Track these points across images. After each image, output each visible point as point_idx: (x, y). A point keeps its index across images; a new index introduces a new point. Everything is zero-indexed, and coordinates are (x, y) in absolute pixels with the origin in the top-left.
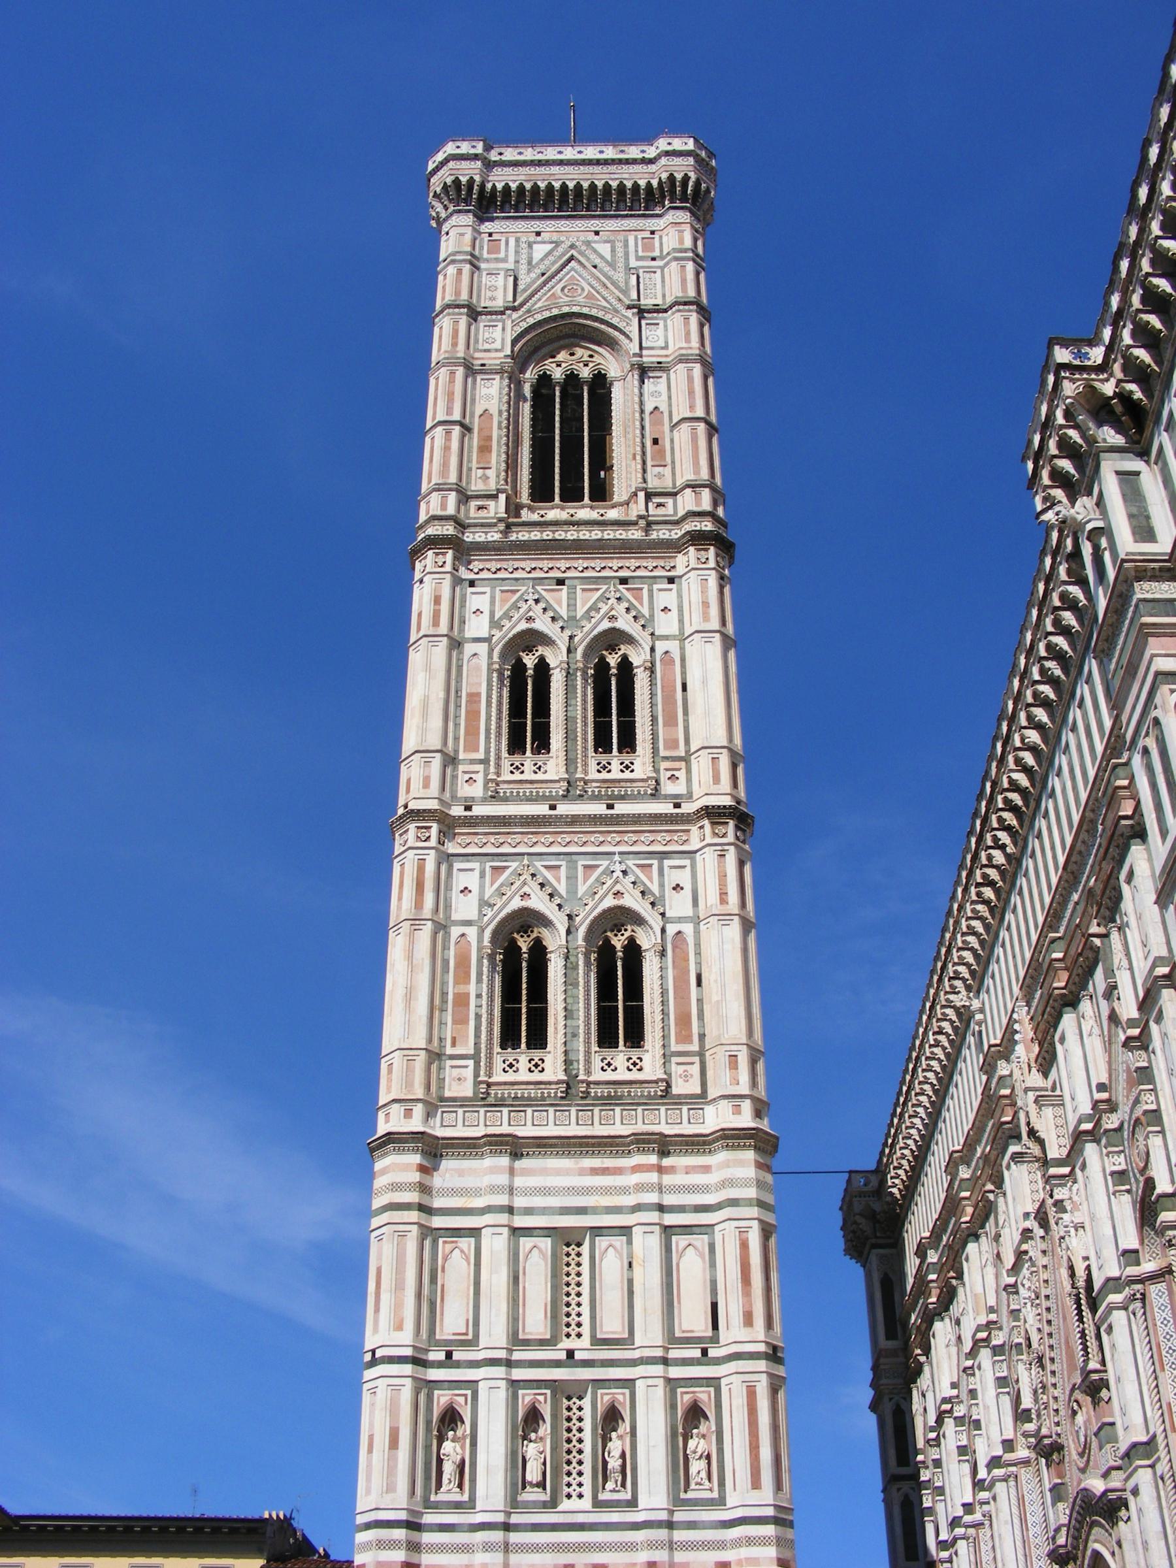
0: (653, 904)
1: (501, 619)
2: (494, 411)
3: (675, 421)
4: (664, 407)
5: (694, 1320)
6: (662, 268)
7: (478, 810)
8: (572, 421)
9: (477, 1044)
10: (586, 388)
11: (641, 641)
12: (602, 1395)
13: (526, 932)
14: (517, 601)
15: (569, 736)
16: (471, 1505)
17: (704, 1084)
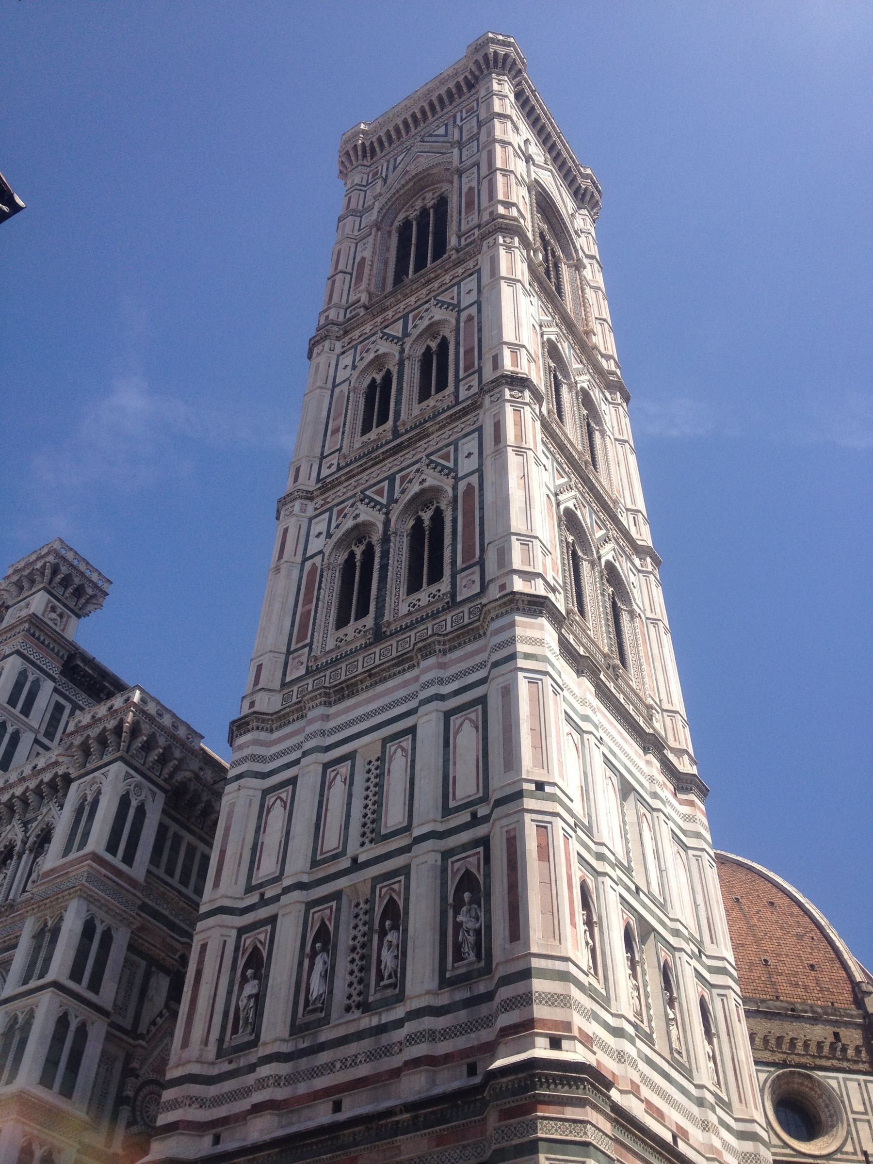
10: (431, 211)
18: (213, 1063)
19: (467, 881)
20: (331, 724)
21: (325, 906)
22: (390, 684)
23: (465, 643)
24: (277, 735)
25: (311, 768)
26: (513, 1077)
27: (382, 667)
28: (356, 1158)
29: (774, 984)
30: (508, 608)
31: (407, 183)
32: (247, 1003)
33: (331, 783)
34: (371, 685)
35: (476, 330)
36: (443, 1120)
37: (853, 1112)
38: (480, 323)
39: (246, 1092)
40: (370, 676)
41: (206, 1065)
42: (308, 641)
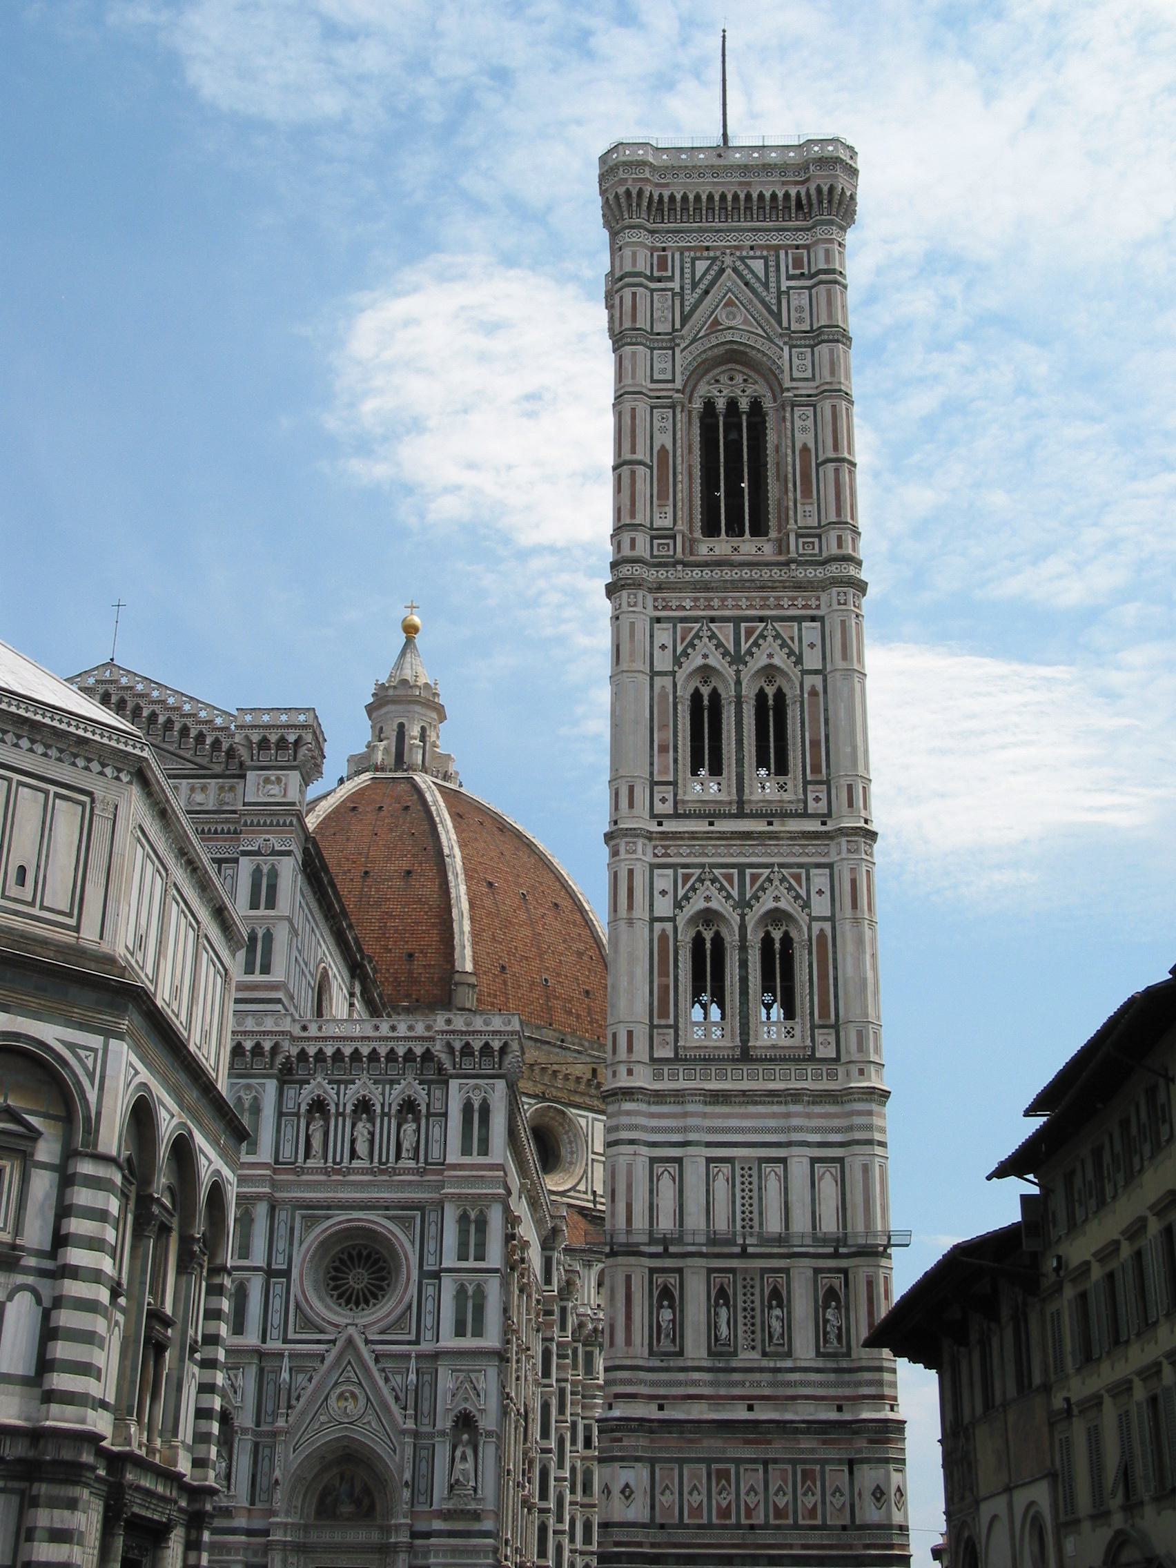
0: (803, 908)
1: (681, 655)
2: (669, 447)
3: (820, 460)
4: (811, 445)
5: (829, 1225)
6: (810, 288)
7: (669, 826)
8: (733, 449)
9: (676, 1017)
10: (744, 417)
11: (794, 678)
12: (768, 1278)
13: (708, 926)
14: (693, 638)
15: (740, 762)
16: (681, 1353)
17: (838, 1051)
19: (831, 1294)
20: (708, 1123)
22: (760, 1109)
24: (655, 1109)
25: (698, 1159)
29: (550, 1009)
30: (868, 1097)
31: (718, 345)
33: (714, 1177)
35: (822, 720)
37: (594, 1153)
38: (826, 710)
39: (679, 1383)
40: (744, 1095)
42: (671, 1022)
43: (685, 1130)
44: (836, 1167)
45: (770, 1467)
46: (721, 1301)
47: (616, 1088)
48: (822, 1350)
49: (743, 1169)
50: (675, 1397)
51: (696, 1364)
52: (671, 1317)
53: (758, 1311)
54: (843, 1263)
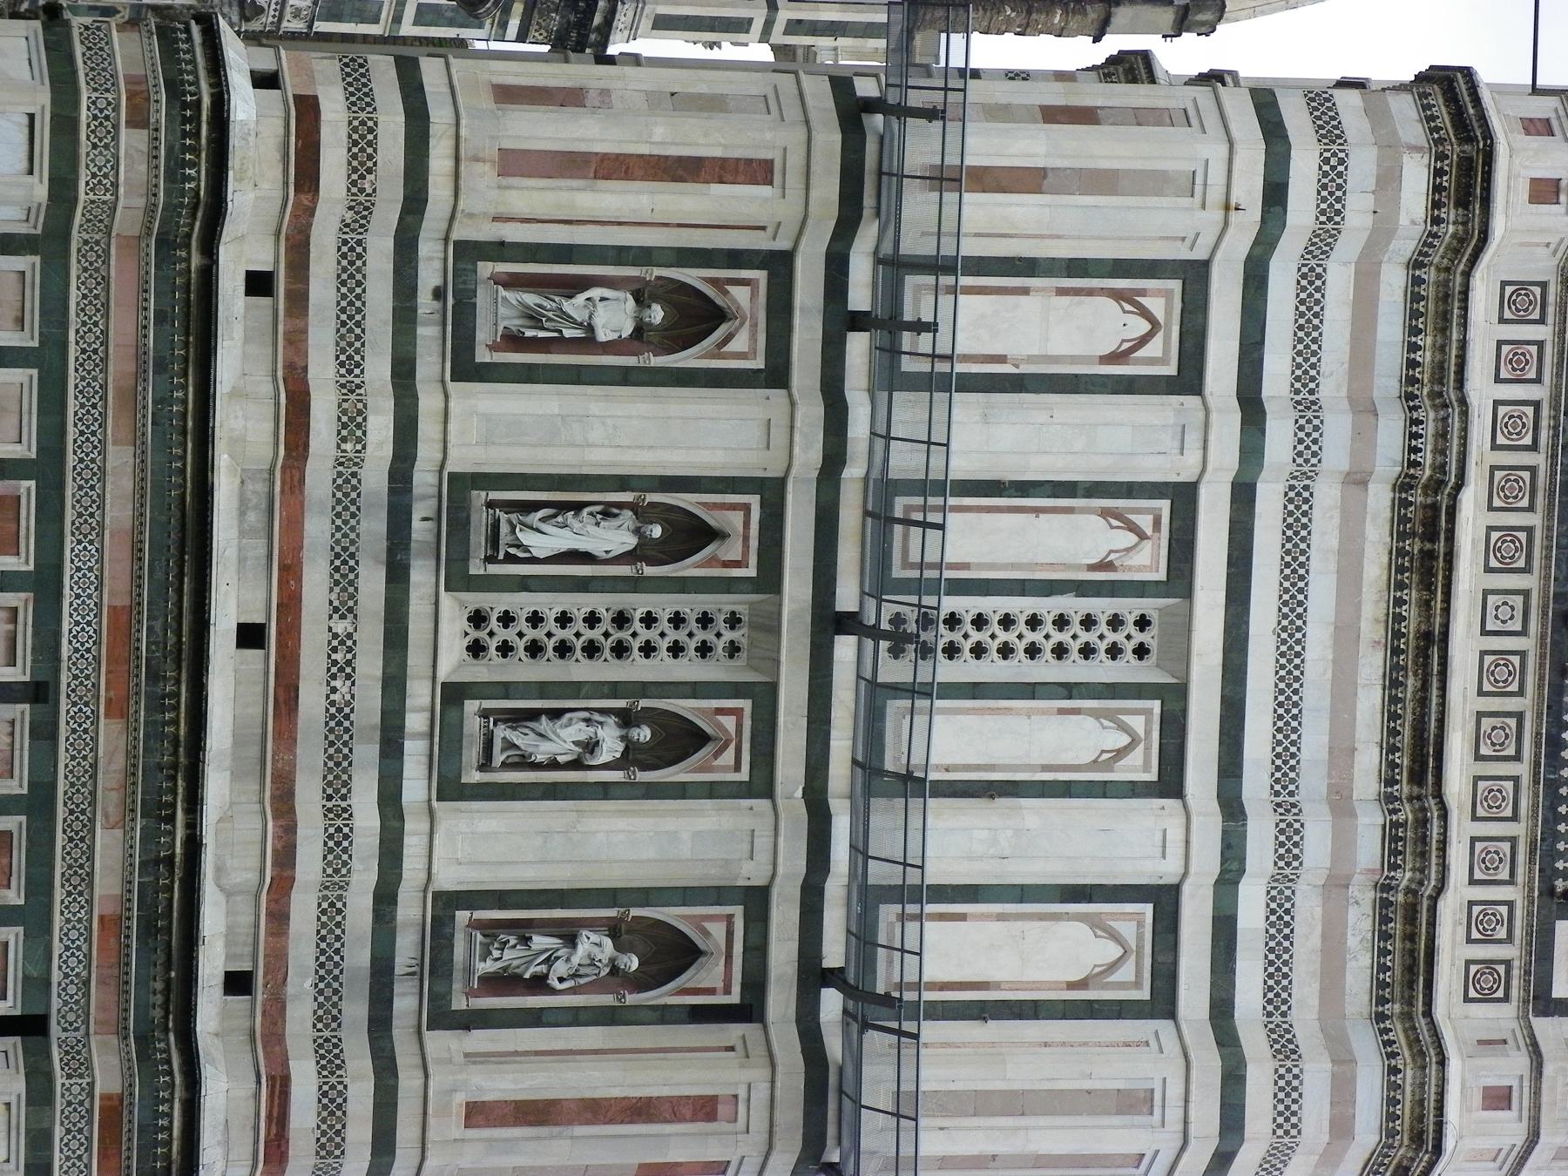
12: (737, 712)
16: (466, 369)
18: (446, 240)
20: (1327, 495)
21: (754, 543)
22: (1370, 701)
23: (1383, 952)
24: (1393, 282)
25: (1193, 458)
26: (176, 1132)
27: (1435, 684)
28: (123, 714)
30: (1404, 1124)
32: (575, 322)
34: (1398, 635)
36: (148, 929)
39: (349, 362)
40: (1426, 637)
41: (444, 226)
43: (1307, 406)
44: (1137, 984)
45: (21, 711)
46: (657, 531)
47: (1488, 135)
48: (462, 916)
49: (1143, 623)
50: (297, 340)
51: (427, 429)
52: (602, 336)
53: (607, 670)
54: (781, 1001)
